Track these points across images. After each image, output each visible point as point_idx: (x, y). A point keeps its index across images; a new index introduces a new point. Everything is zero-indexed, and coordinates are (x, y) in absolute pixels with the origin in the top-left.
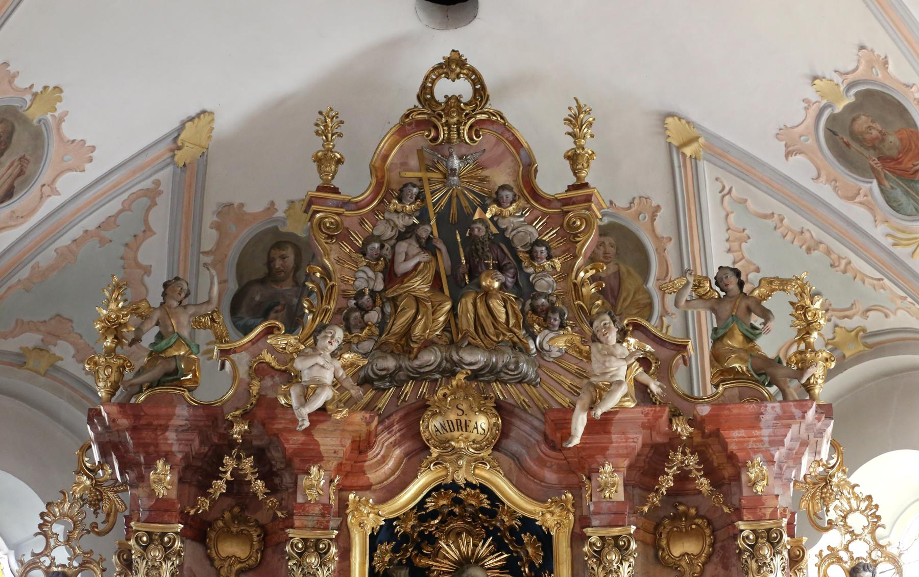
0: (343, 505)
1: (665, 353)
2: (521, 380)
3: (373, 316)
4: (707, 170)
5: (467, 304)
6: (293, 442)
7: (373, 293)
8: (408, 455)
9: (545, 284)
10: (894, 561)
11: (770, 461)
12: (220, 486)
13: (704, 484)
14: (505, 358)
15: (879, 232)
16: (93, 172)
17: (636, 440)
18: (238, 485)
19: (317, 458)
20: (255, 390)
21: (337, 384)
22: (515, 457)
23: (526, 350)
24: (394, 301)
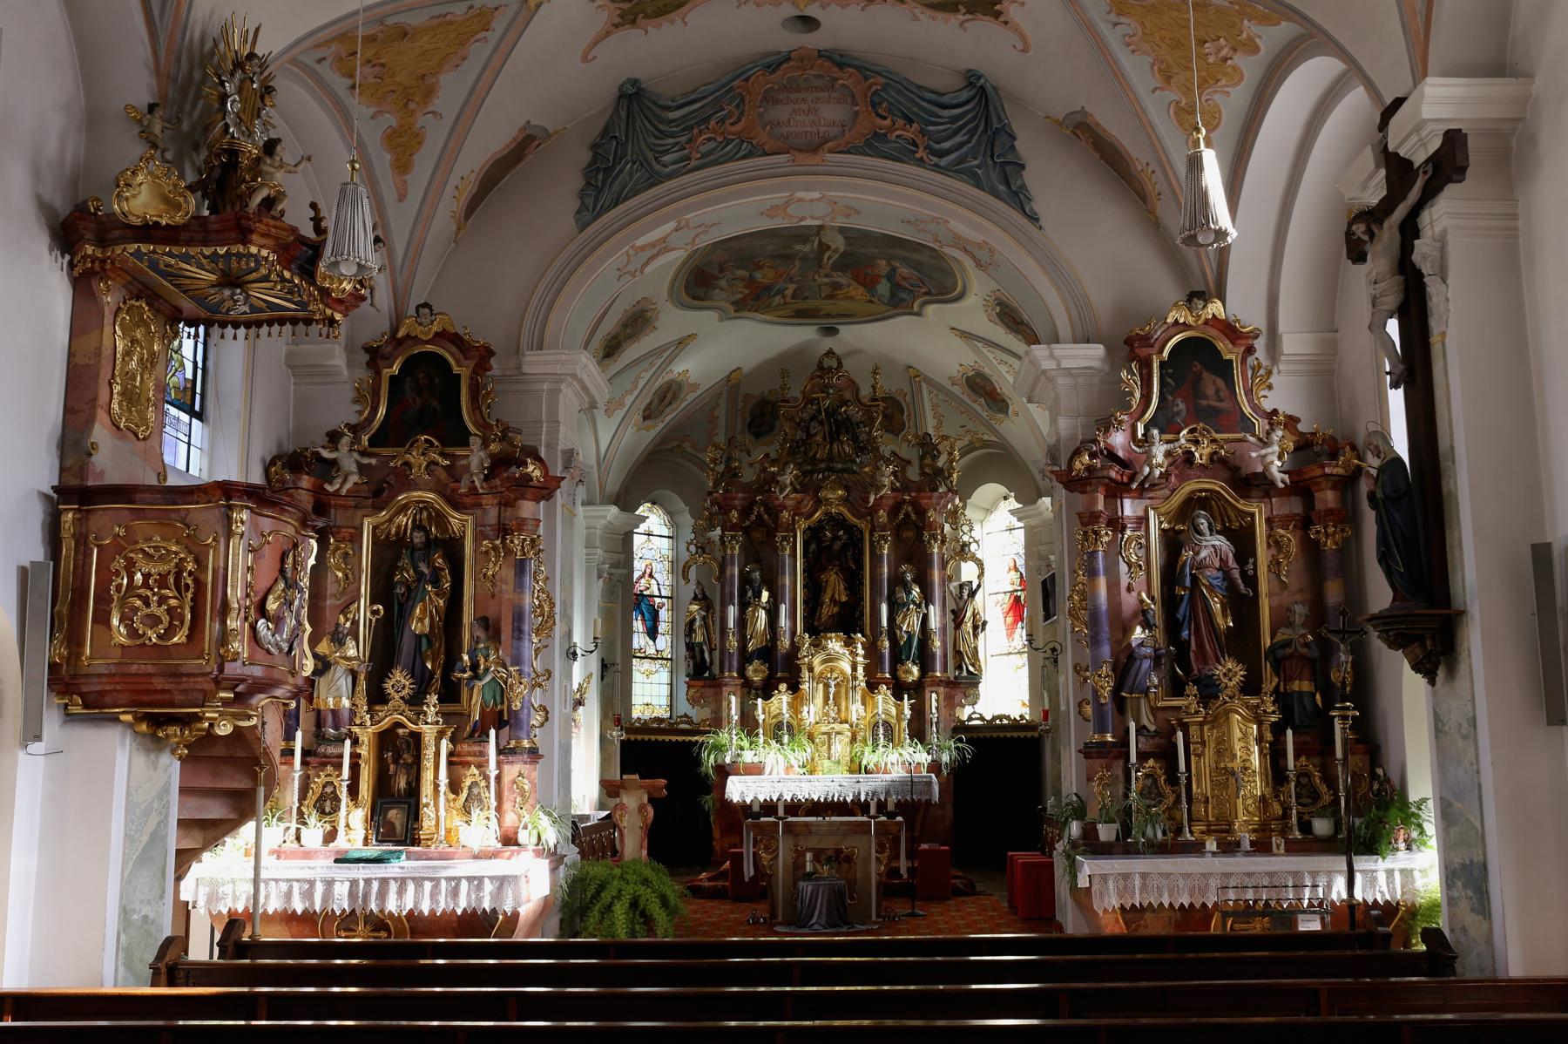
0: (794, 520)
1: (903, 463)
2: (855, 472)
3: (802, 449)
4: (924, 385)
5: (835, 446)
6: (776, 503)
7: (802, 440)
8: (815, 502)
9: (863, 437)
10: (977, 542)
11: (935, 510)
12: (753, 517)
13: (914, 517)
14: (849, 465)
15: (984, 414)
16: (699, 392)
17: (891, 502)
18: (759, 516)
19: (785, 508)
20: (762, 477)
21: (791, 484)
22: (851, 503)
23: (855, 462)
24: (810, 444)
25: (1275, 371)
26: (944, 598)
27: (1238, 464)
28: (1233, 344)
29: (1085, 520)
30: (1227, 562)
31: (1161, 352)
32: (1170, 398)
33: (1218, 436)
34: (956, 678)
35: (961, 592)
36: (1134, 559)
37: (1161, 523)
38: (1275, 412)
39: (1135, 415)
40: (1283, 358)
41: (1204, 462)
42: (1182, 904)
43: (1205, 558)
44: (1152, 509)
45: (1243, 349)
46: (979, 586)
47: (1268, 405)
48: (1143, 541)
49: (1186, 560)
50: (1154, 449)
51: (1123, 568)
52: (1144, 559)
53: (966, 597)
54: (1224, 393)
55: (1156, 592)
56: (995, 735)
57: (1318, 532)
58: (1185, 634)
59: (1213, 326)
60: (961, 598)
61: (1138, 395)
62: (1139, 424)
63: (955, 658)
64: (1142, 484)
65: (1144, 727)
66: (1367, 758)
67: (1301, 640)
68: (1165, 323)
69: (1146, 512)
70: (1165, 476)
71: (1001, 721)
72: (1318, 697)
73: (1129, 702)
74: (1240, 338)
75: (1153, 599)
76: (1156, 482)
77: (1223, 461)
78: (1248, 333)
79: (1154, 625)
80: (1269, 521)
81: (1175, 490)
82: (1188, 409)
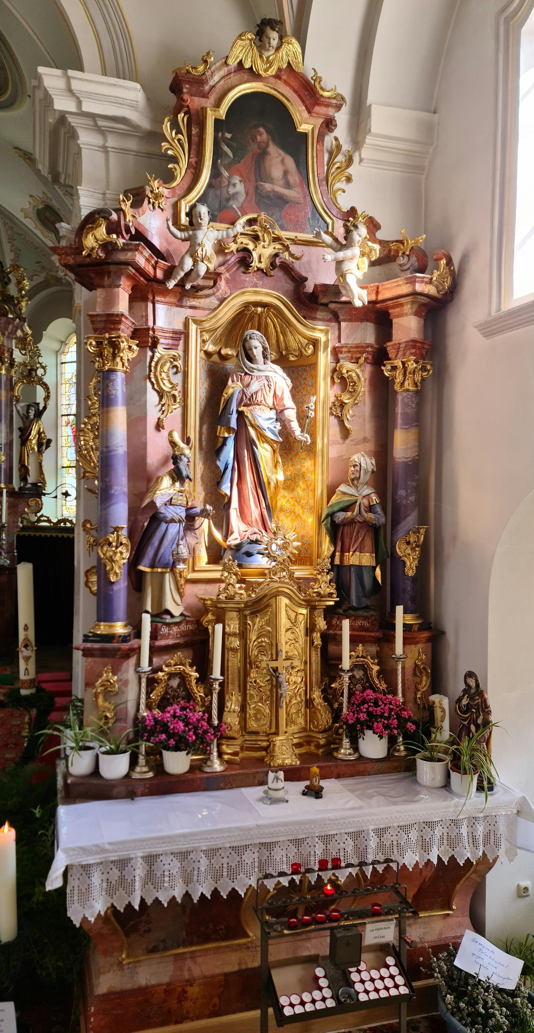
25: (356, 158)
26: (12, 416)
27: (304, 274)
28: (309, 112)
29: (101, 325)
30: (282, 399)
31: (218, 104)
32: (226, 174)
33: (284, 234)
34: (20, 488)
35: (28, 412)
36: (166, 387)
37: (204, 342)
38: (353, 212)
39: (179, 192)
40: (369, 140)
41: (262, 266)
42: (203, 895)
43: (256, 393)
44: (195, 321)
45: (320, 121)
46: (45, 408)
47: (345, 203)
48: (179, 363)
49: (232, 395)
50: (200, 234)
51: (152, 397)
52: (179, 388)
53: (32, 417)
54: (294, 178)
55: (193, 433)
56: (60, 535)
57: (394, 368)
58: (225, 488)
59: (286, 83)
60: (28, 417)
61: (184, 164)
62: (183, 203)
63: (20, 470)
64: (181, 284)
65: (168, 612)
66: (430, 645)
67: (365, 501)
68: (226, 64)
69: (186, 324)
70: (213, 276)
71: (65, 524)
72: (378, 572)
73: (148, 578)
74: (319, 105)
75: (187, 441)
76: (200, 282)
77: (286, 268)
78: (329, 98)
79: (188, 477)
80: (336, 352)
81: (225, 299)
82: (247, 194)
